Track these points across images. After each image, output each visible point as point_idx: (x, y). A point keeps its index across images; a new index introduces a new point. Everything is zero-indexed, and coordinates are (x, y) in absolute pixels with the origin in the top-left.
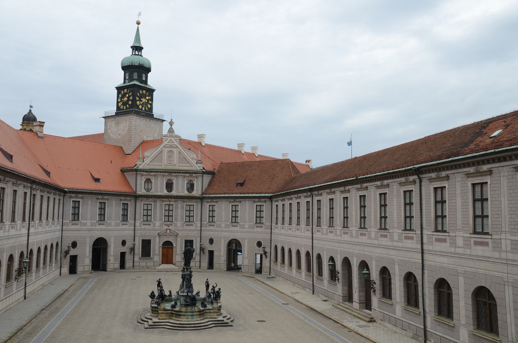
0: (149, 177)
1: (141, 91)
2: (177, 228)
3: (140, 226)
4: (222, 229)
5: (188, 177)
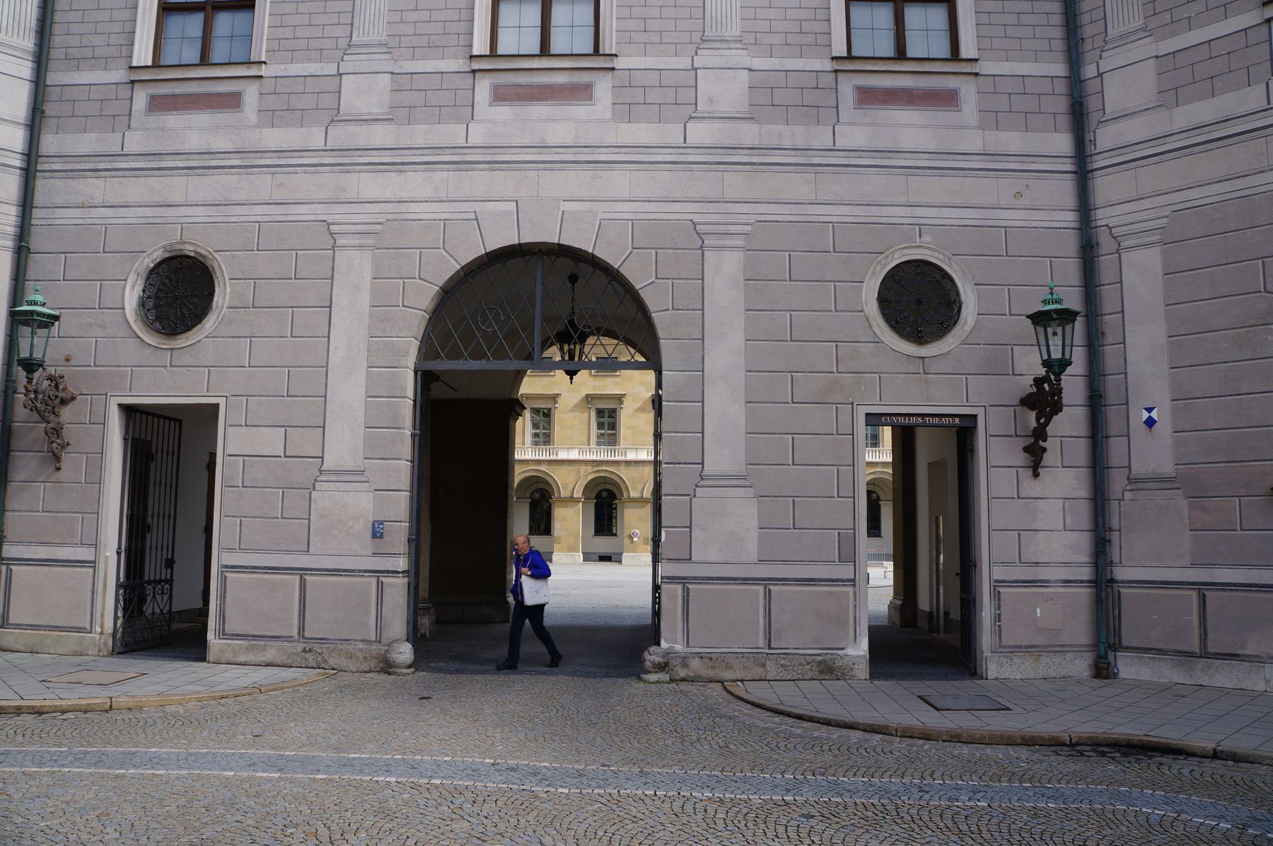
4: (343, 135)
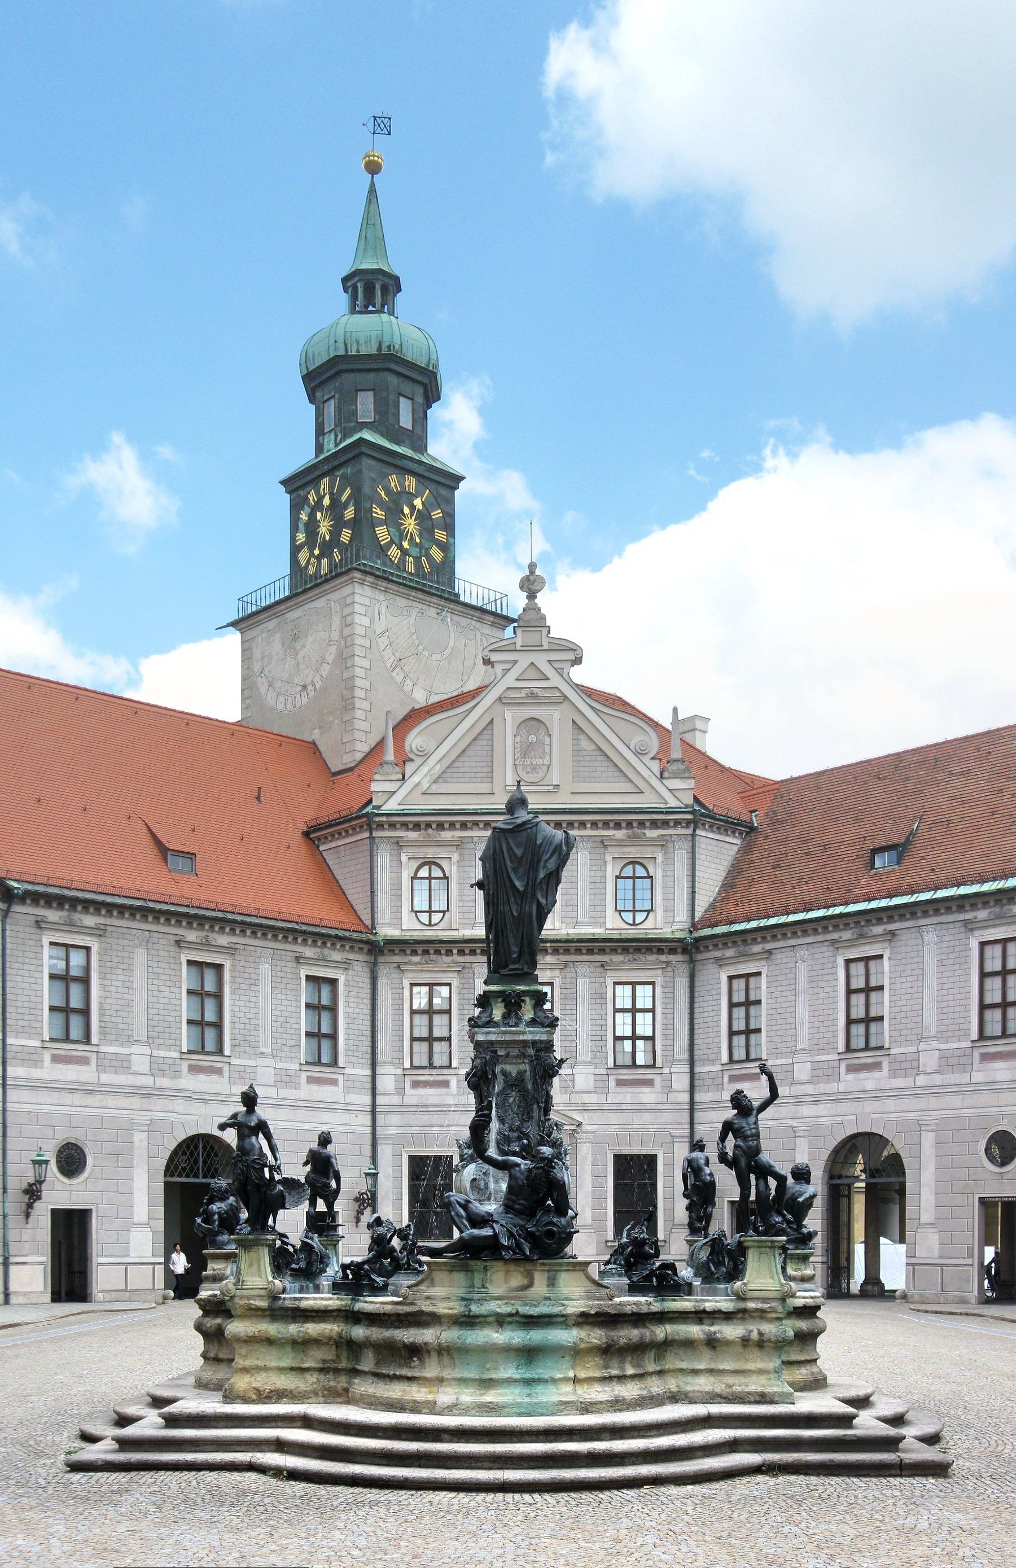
0: (431, 853)
1: (393, 481)
2: (575, 1098)
5: (620, 844)
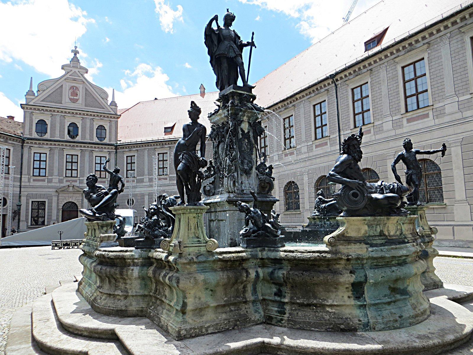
3: (29, 181)
